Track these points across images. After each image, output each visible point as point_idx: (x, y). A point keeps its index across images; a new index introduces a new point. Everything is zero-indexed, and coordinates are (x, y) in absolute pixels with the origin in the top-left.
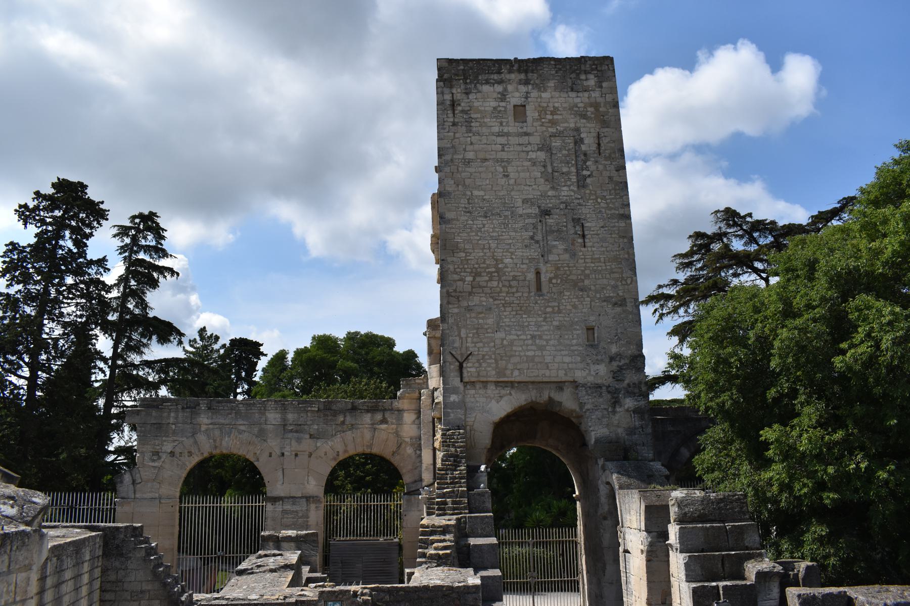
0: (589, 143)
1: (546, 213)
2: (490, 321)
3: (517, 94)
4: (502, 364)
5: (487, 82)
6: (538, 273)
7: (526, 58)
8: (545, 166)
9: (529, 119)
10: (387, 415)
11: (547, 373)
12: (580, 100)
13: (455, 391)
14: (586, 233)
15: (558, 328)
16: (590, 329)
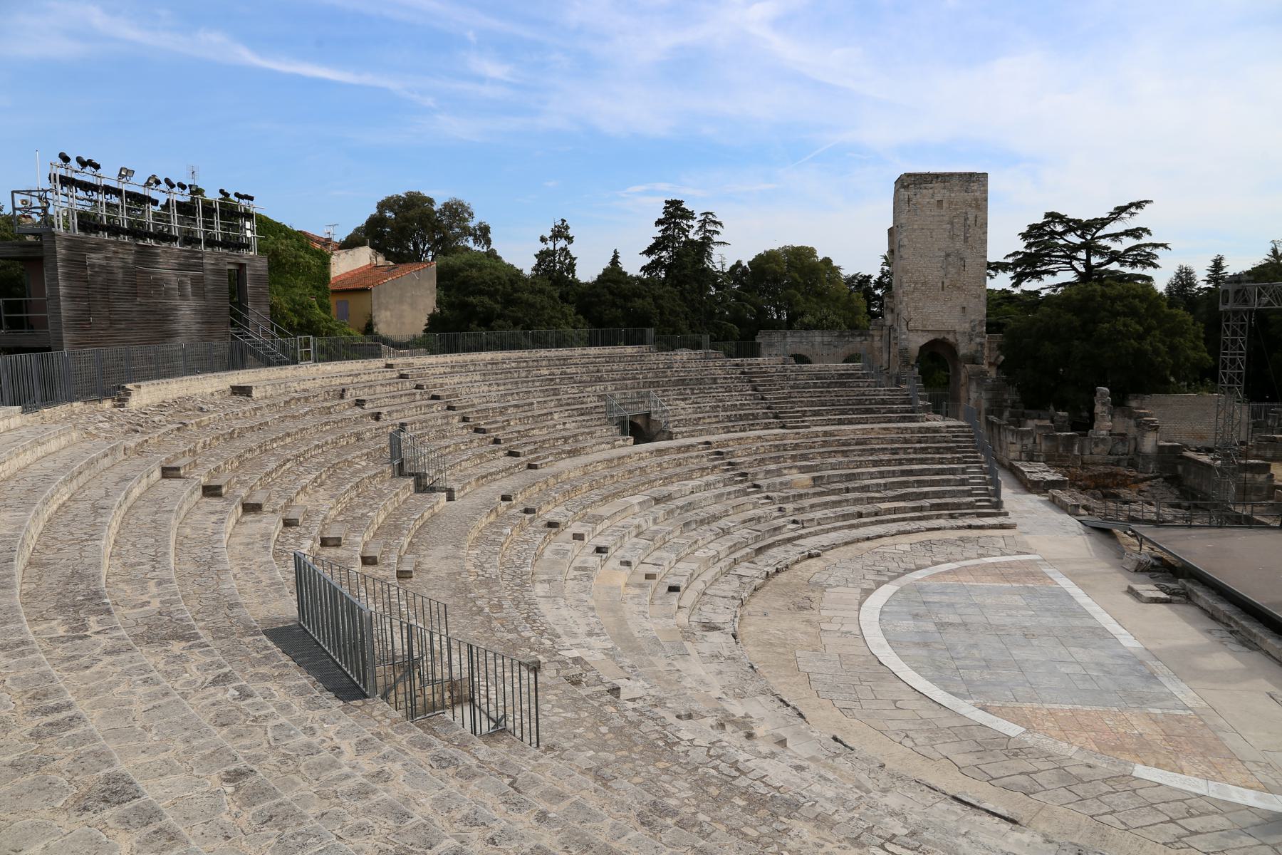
1: (948, 255)
12: (969, 197)
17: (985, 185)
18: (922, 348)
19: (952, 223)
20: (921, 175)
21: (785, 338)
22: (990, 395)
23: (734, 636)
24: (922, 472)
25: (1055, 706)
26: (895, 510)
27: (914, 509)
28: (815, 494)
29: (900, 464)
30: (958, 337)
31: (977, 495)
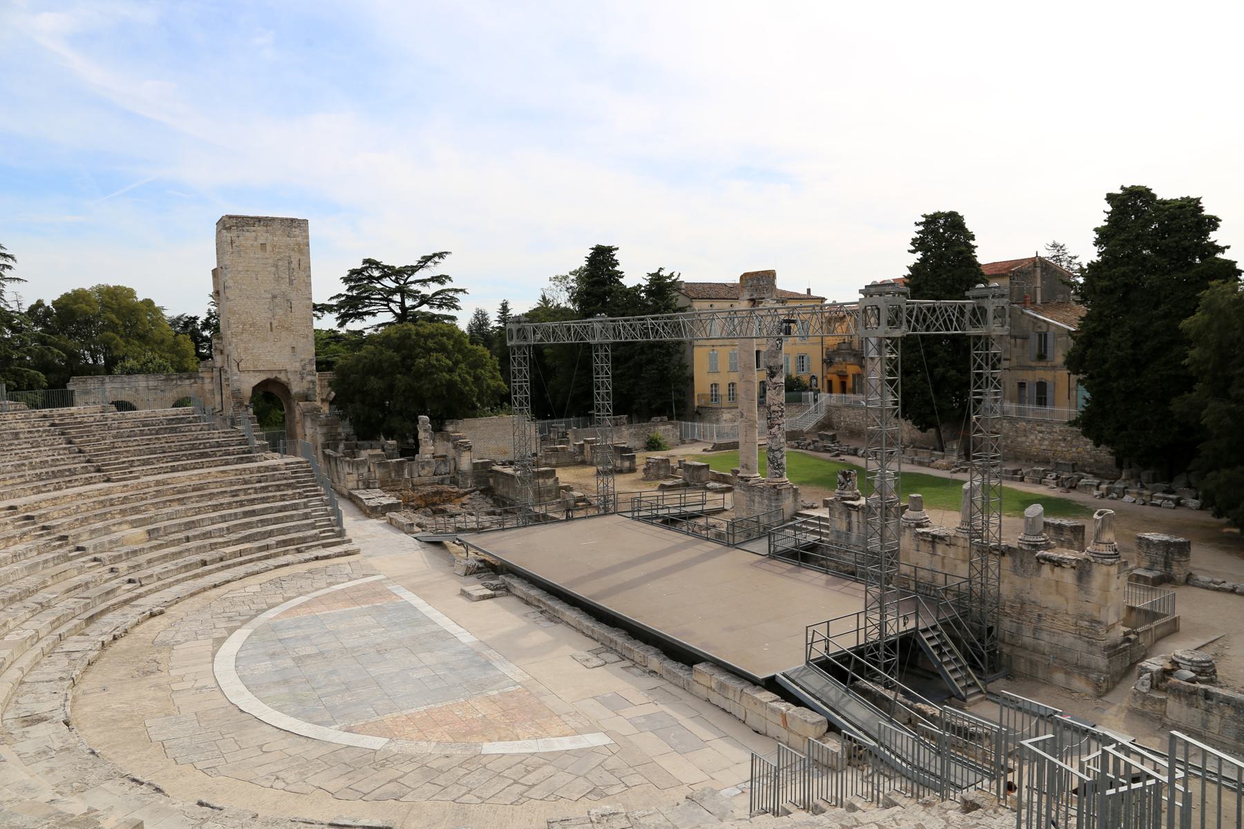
0: (295, 264)
1: (274, 297)
12: (291, 241)
17: (306, 231)
18: (255, 389)
20: (243, 217)
21: (103, 383)
22: (324, 430)
23: (67, 723)
24: (264, 511)
25: (412, 711)
26: (241, 553)
27: (260, 549)
28: (152, 548)
29: (242, 505)
30: (290, 376)
31: (321, 527)
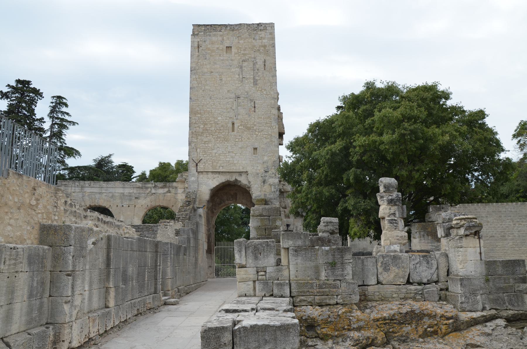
2: (210, 145)
3: (228, 41)
4: (215, 164)
5: (215, 35)
6: (233, 124)
7: (234, 24)
8: (239, 75)
9: (233, 53)
10: (171, 189)
11: (235, 168)
13: (193, 175)
14: (256, 105)
15: (241, 148)
16: (255, 149)
17: (272, 34)
19: (241, 67)
30: (251, 178)
